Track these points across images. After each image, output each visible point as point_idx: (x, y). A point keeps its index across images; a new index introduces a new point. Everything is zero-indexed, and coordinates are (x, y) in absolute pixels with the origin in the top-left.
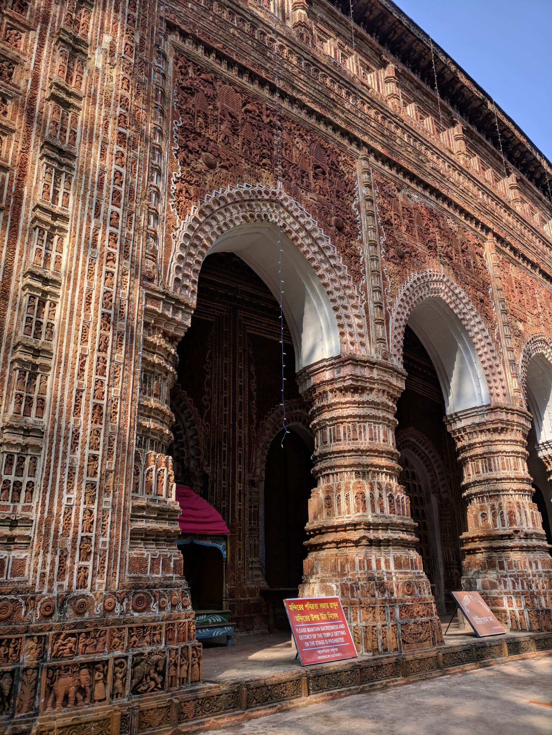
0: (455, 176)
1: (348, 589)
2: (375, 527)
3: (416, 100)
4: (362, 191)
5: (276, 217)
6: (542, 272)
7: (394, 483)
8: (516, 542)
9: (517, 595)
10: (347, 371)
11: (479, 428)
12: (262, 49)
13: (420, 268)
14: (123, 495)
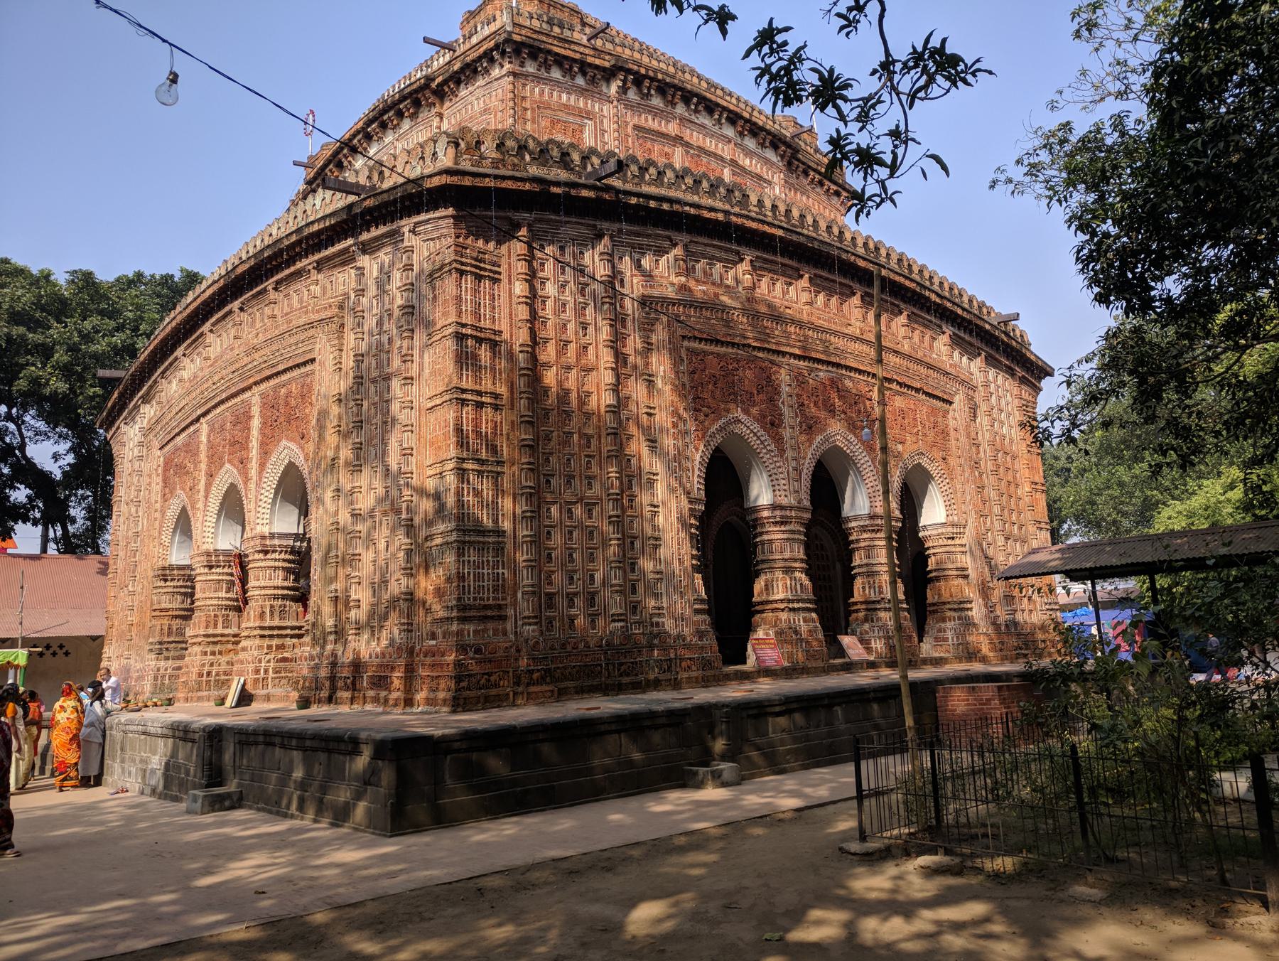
0: (853, 346)
1: (779, 633)
3: (824, 289)
4: (785, 389)
5: (740, 429)
7: (803, 576)
8: (882, 605)
10: (778, 513)
11: (864, 529)
12: (728, 323)
13: (823, 430)
14: (690, 596)
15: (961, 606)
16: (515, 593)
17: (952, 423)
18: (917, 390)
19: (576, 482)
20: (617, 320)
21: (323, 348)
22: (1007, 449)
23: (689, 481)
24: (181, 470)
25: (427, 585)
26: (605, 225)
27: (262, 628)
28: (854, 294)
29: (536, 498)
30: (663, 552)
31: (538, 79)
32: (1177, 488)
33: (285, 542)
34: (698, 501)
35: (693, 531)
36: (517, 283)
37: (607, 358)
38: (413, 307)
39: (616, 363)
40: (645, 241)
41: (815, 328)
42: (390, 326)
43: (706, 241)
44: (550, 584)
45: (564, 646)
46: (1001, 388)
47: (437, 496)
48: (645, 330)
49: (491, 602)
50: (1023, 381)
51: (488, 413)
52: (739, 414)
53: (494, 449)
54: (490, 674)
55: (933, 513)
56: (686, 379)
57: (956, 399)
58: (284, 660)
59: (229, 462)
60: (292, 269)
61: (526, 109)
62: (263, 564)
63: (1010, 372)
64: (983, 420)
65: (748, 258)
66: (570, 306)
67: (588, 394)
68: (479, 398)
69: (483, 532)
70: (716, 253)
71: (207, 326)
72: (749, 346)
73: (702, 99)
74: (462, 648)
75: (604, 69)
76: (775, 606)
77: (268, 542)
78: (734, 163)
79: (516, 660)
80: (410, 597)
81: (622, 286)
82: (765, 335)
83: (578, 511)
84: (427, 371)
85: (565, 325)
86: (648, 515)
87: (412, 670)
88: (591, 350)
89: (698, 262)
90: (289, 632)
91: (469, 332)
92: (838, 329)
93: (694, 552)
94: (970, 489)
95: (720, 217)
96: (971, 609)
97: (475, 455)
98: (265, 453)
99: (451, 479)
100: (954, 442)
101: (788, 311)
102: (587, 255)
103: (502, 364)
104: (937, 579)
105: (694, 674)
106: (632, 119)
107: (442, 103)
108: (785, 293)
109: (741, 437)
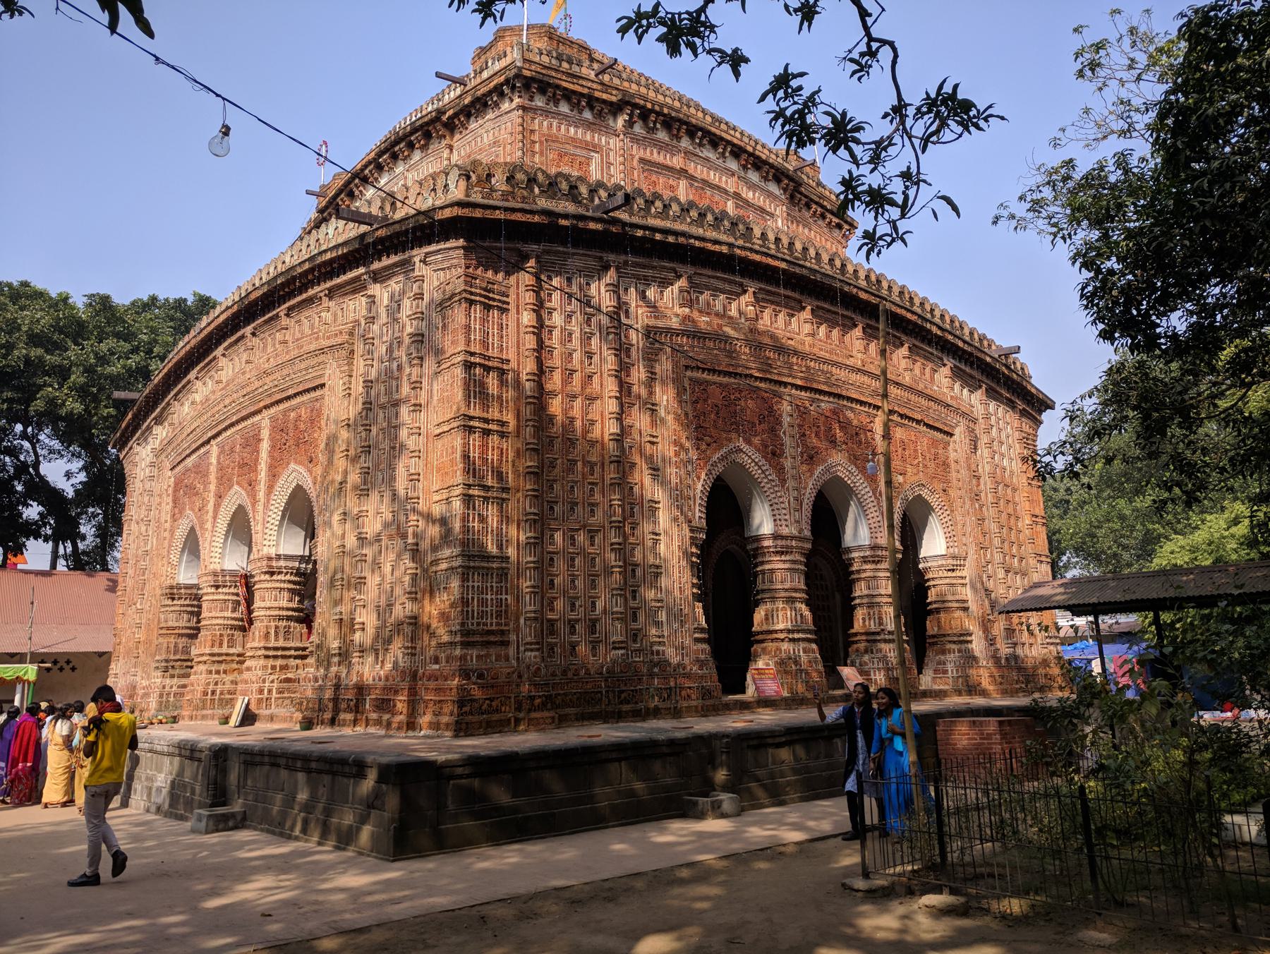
0: (854, 377)
1: (781, 663)
2: (792, 631)
3: (827, 320)
4: (786, 420)
6: (926, 424)
7: (803, 606)
9: (879, 669)
10: (779, 542)
11: (865, 560)
12: (731, 354)
15: (963, 638)
16: (517, 619)
17: (952, 455)
18: (918, 422)
19: (579, 509)
20: (622, 350)
21: (333, 374)
22: (1008, 481)
23: (690, 510)
24: (192, 491)
25: (432, 610)
26: (612, 257)
27: (266, 648)
28: (856, 326)
29: (540, 523)
30: (664, 582)
31: (546, 113)
32: (1179, 522)
33: (290, 564)
34: (699, 530)
35: (694, 559)
36: (525, 313)
37: (611, 386)
38: (423, 335)
39: (620, 392)
40: (650, 273)
41: (817, 359)
42: (401, 354)
43: (710, 273)
44: (552, 610)
45: (564, 672)
46: (1002, 421)
47: (443, 521)
48: (649, 360)
49: (494, 628)
50: (1023, 413)
51: (494, 440)
52: (741, 444)
53: (500, 476)
54: (491, 700)
55: (934, 545)
56: (689, 409)
57: (957, 431)
58: (288, 680)
59: (238, 483)
60: (304, 296)
61: (534, 142)
62: (269, 585)
63: (1011, 404)
64: (983, 452)
65: (751, 290)
66: (576, 335)
67: (593, 422)
68: (486, 426)
69: (488, 557)
70: (720, 285)
71: (220, 349)
72: (752, 376)
73: (706, 133)
74: (465, 674)
75: (611, 104)
76: (775, 636)
77: (274, 564)
78: (737, 196)
79: (518, 685)
80: (414, 620)
81: (627, 317)
82: (767, 366)
83: (581, 538)
84: (435, 398)
85: (571, 354)
86: (650, 543)
87: (415, 694)
88: (596, 379)
89: (702, 293)
90: (292, 652)
91: (478, 360)
92: (840, 360)
93: (695, 581)
94: (971, 520)
95: (725, 249)
96: (971, 642)
97: (480, 483)
98: (273, 476)
99: (457, 504)
100: (954, 474)
101: (790, 342)
102: (594, 286)
103: (510, 394)
104: (938, 611)
105: (694, 703)
106: (638, 152)
107: (452, 135)
108: (788, 324)
109: (742, 466)
